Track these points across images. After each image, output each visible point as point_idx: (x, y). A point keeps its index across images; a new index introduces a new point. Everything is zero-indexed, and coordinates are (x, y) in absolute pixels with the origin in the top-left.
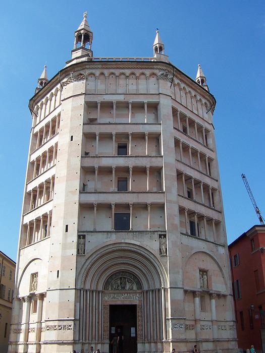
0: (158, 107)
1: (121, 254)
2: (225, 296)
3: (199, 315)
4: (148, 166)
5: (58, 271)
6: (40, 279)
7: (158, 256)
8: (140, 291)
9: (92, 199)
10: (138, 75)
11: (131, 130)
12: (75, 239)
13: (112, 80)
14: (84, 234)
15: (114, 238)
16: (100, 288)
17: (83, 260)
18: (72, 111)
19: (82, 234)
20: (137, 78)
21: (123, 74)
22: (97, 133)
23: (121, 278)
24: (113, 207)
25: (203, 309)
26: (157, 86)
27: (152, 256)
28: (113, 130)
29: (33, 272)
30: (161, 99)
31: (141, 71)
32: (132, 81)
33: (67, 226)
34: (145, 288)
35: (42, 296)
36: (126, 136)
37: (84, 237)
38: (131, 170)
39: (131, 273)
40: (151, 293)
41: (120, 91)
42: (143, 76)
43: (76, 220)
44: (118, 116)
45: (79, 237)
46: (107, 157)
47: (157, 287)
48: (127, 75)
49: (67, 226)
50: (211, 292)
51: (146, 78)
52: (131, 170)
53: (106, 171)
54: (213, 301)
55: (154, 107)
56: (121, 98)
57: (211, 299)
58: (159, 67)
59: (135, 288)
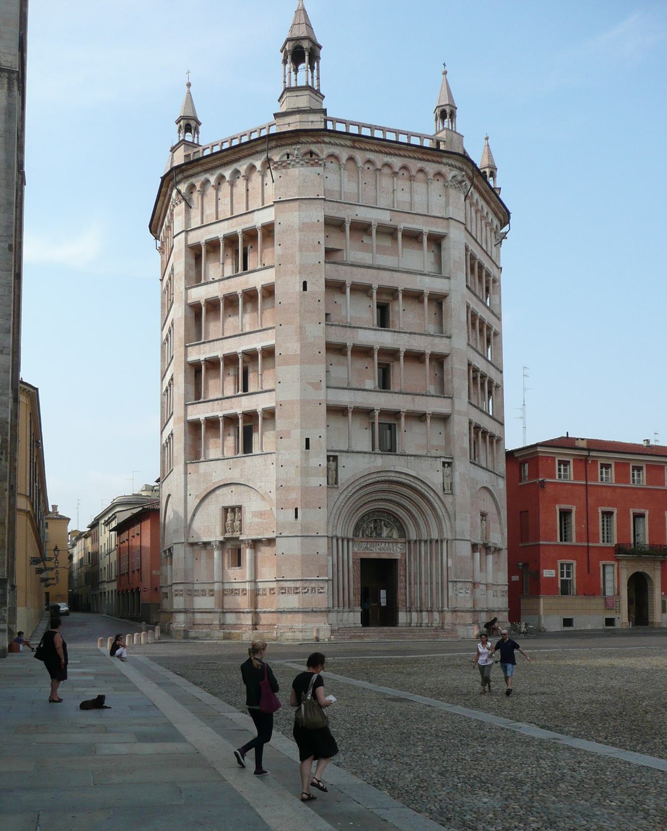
0: (444, 244)
1: (385, 486)
2: (500, 550)
3: (479, 577)
4: (428, 352)
5: (296, 509)
6: (248, 517)
7: (440, 493)
8: (403, 540)
9: (346, 399)
10: (414, 172)
11: (403, 282)
12: (324, 462)
13: (368, 177)
14: (336, 454)
15: (380, 462)
16: (351, 536)
17: (336, 493)
18: (300, 230)
19: (332, 454)
20: (411, 178)
21: (387, 165)
22: (348, 284)
23: (375, 521)
24: (377, 413)
25: (481, 570)
26: (443, 199)
27: (432, 493)
28: (376, 279)
29: (227, 504)
30: (451, 229)
31: (420, 164)
32: (401, 183)
33: (307, 440)
34: (413, 536)
35: (255, 544)
36: (393, 292)
37: (335, 458)
38: (402, 355)
39: (389, 513)
40: (423, 544)
41: (382, 203)
42: (420, 176)
43: (323, 431)
44: (381, 250)
45: (328, 457)
46: (366, 328)
47: (435, 535)
48: (396, 170)
49: (307, 440)
50: (490, 545)
51: (427, 182)
52: (402, 355)
53: (363, 352)
54: (490, 557)
55: (437, 241)
56: (385, 217)
57: (487, 554)
58: (450, 161)
59: (395, 535)
